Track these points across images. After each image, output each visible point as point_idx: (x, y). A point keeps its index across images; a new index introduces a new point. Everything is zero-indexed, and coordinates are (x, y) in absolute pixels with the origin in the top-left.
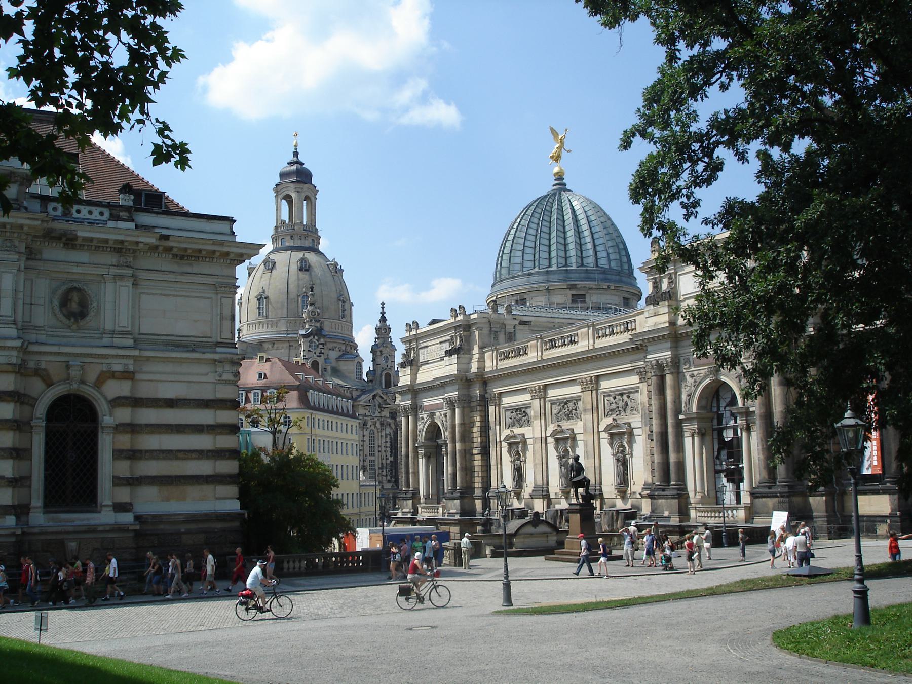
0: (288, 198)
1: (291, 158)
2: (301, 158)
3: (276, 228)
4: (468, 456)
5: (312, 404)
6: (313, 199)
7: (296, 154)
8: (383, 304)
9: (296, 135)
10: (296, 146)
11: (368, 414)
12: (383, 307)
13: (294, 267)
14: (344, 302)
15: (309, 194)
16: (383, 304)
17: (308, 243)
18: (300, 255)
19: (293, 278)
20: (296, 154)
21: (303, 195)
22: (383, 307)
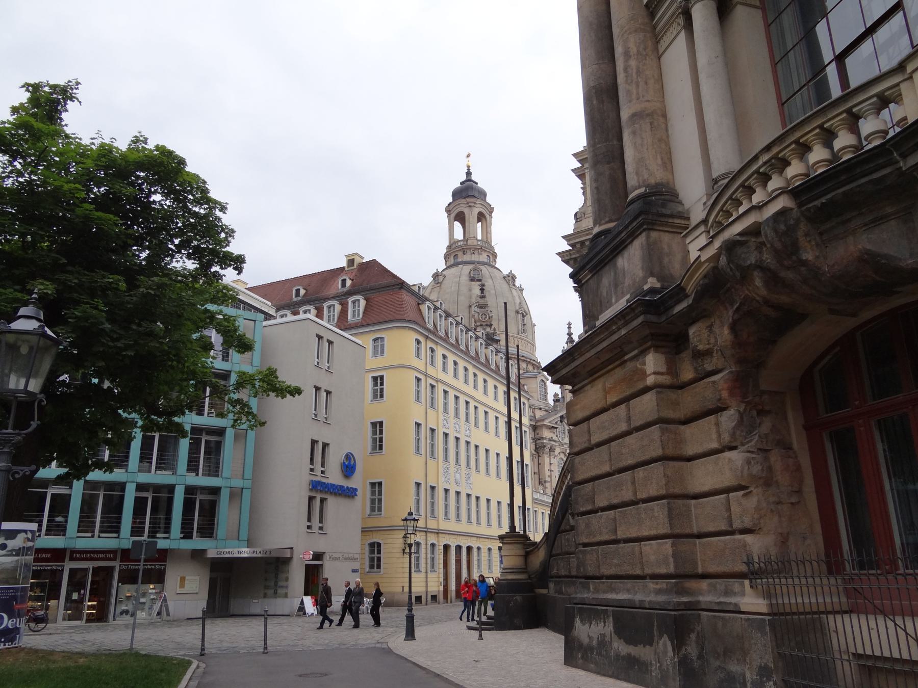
0: (460, 218)
1: (464, 178)
2: (473, 178)
3: (449, 247)
5: (430, 326)
6: (488, 216)
7: (469, 174)
8: (569, 324)
9: (468, 156)
10: (469, 167)
11: (555, 438)
12: (569, 328)
13: (465, 279)
14: (524, 316)
15: (484, 212)
16: (569, 324)
17: (483, 258)
18: (471, 267)
19: (464, 289)
20: (469, 174)
21: (476, 211)
22: (569, 328)
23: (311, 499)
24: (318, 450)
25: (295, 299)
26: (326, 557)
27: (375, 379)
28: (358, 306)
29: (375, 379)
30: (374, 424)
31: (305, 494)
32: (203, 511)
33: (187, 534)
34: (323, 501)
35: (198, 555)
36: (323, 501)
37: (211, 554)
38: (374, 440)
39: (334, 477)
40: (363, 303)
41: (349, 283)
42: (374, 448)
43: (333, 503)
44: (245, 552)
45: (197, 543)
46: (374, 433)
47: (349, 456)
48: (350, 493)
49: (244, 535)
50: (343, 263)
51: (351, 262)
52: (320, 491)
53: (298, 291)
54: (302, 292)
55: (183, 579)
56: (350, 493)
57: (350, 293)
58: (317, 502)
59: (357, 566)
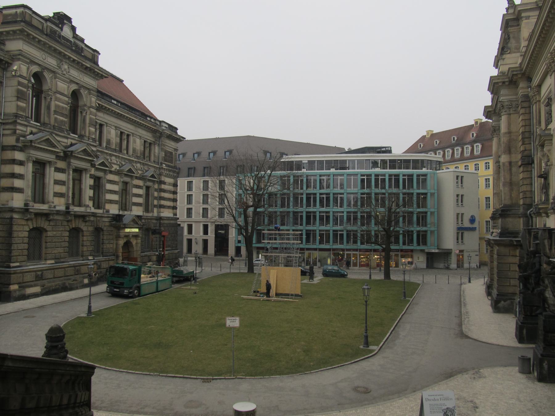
4: (514, 169)
23: (458, 233)
24: (459, 216)
25: (453, 142)
26: (465, 251)
27: (486, 179)
28: (478, 148)
29: (486, 179)
30: (486, 198)
31: (456, 232)
32: (423, 238)
33: (418, 244)
34: (462, 233)
35: (422, 251)
36: (462, 233)
37: (426, 251)
38: (487, 204)
39: (467, 224)
40: (480, 146)
41: (475, 135)
42: (487, 207)
43: (466, 234)
44: (437, 251)
45: (422, 247)
46: (487, 201)
47: (472, 216)
48: (474, 229)
49: (436, 245)
50: (473, 123)
51: (476, 123)
52: (461, 231)
53: (454, 138)
54: (456, 138)
55: (418, 258)
56: (474, 229)
57: (475, 141)
58: (460, 234)
59: (478, 253)
